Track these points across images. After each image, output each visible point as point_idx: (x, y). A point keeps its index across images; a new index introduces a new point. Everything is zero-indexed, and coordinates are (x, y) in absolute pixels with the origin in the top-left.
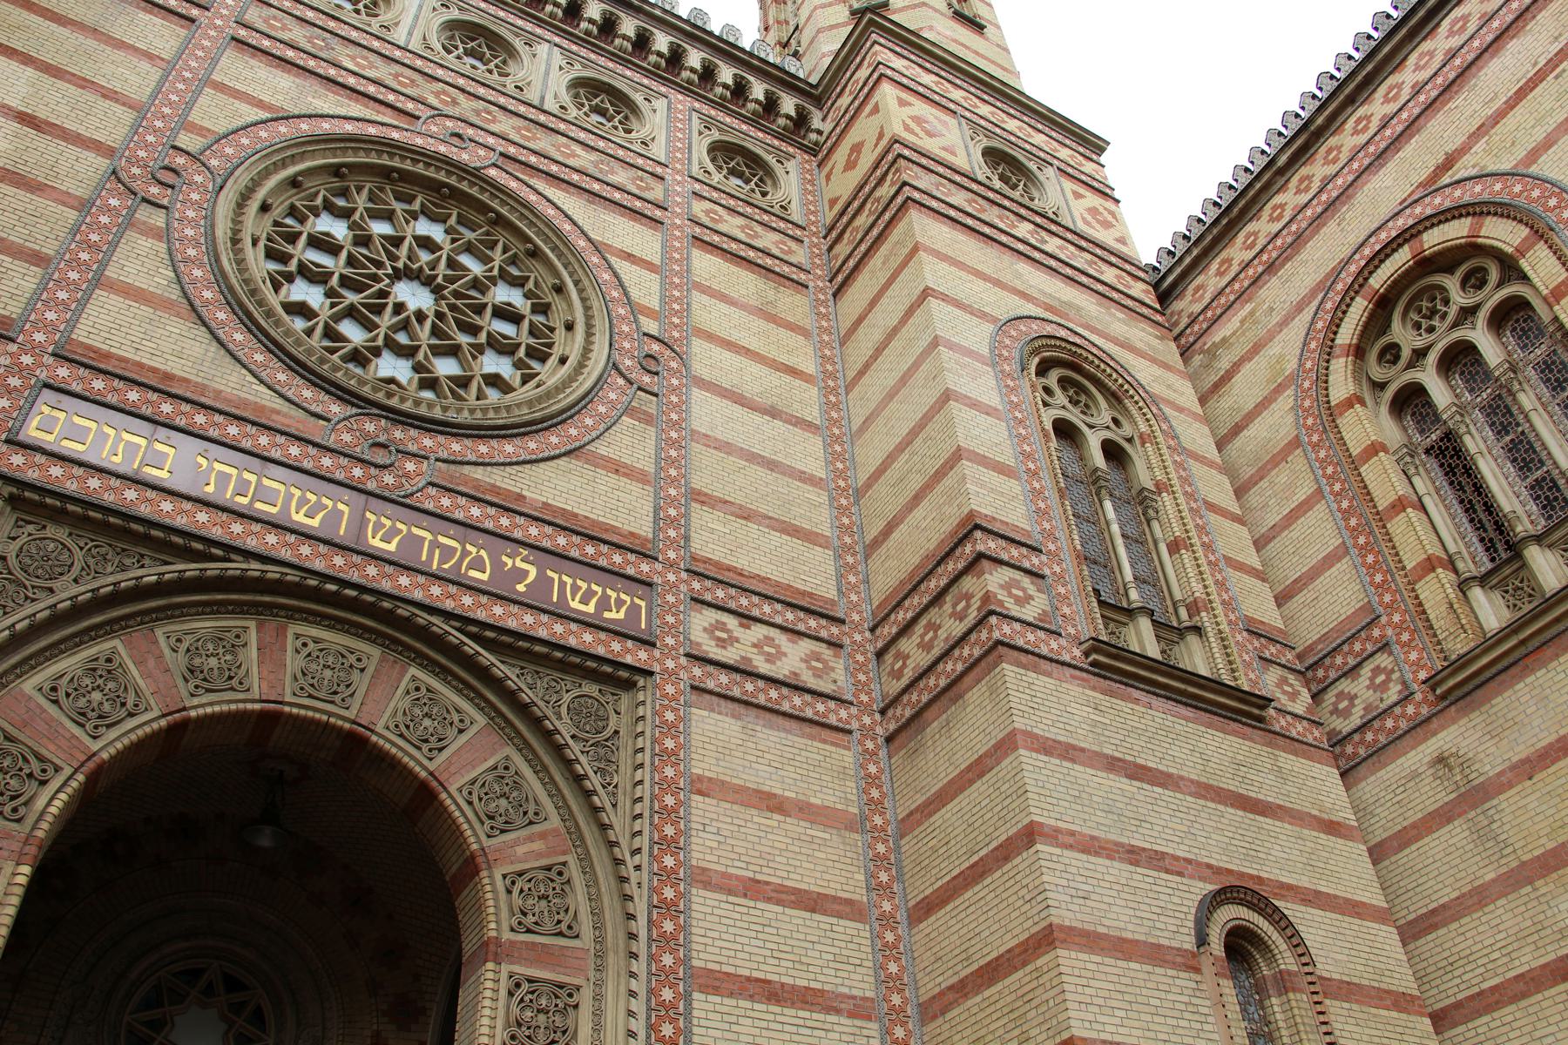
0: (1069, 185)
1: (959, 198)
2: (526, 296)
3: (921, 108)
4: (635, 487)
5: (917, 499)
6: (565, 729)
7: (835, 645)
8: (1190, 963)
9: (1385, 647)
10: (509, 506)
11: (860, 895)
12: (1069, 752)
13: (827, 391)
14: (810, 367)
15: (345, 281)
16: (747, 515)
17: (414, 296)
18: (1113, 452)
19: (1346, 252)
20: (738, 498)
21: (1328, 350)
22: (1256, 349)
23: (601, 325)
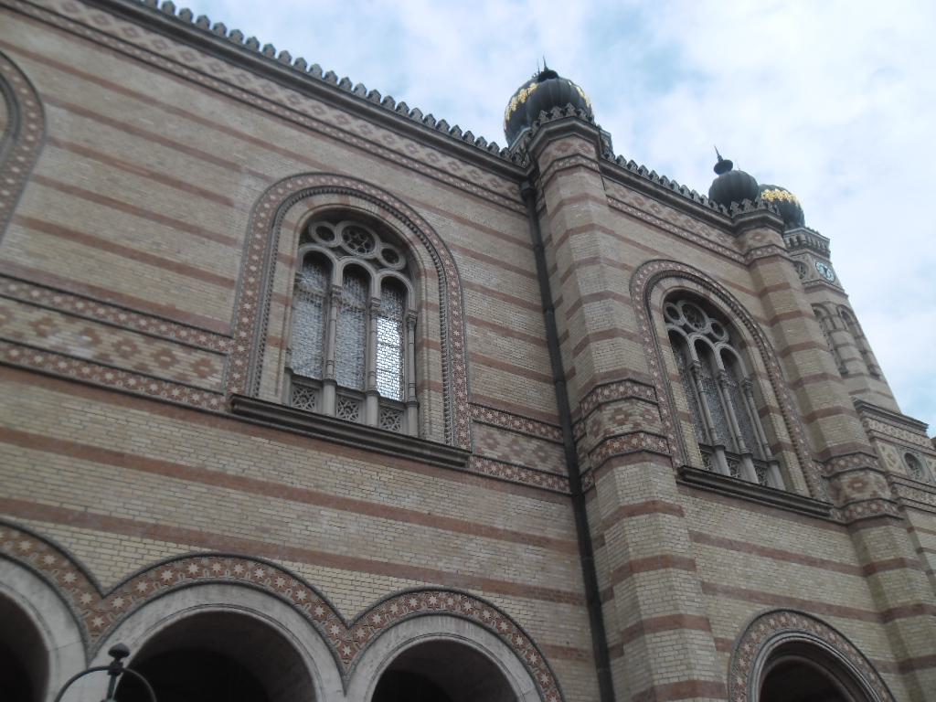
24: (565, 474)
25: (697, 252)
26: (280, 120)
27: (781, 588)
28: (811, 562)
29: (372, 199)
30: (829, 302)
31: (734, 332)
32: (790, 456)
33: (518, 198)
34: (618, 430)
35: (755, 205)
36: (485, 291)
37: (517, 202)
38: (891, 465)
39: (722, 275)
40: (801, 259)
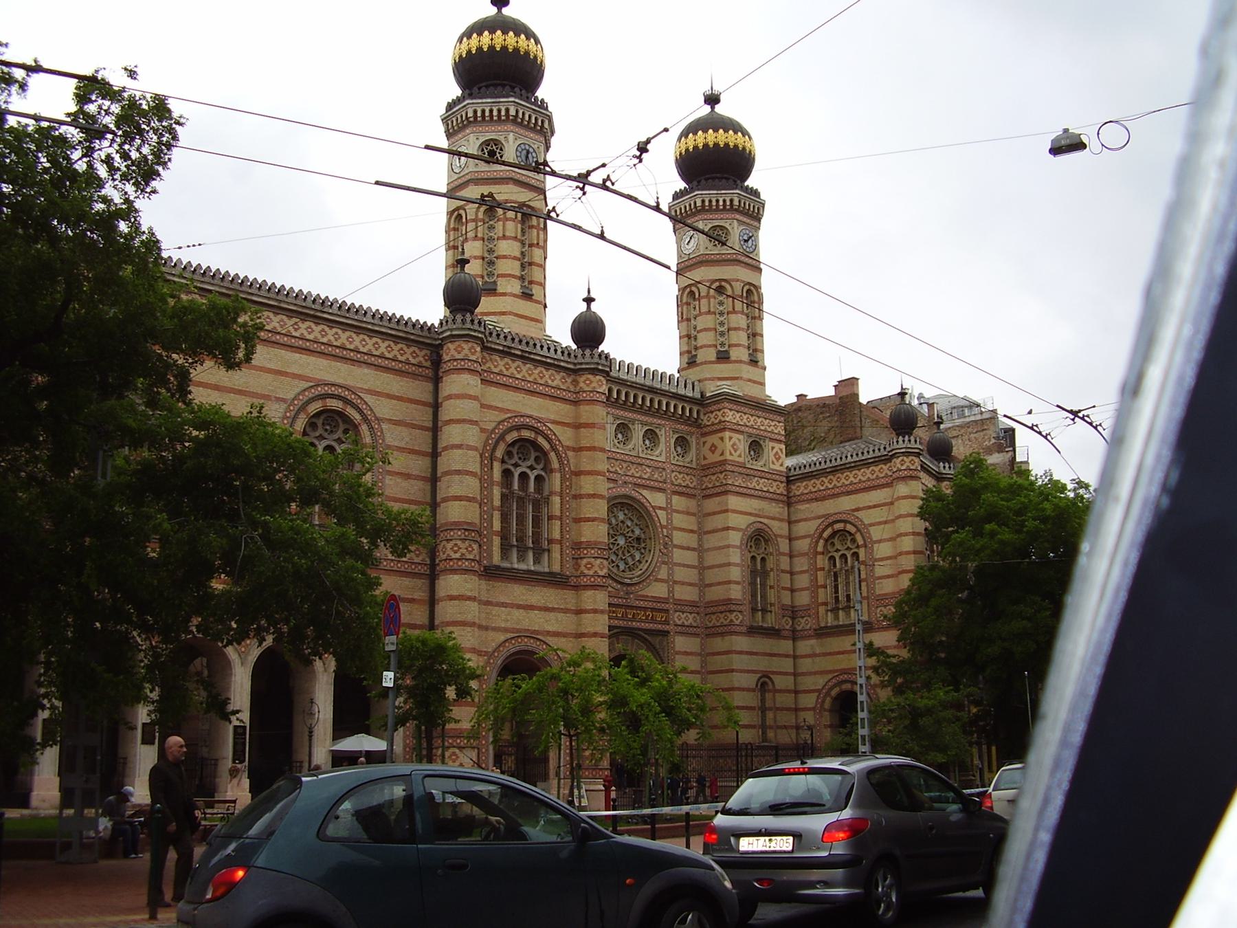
0: (771, 444)
1: (739, 482)
2: (641, 529)
3: (736, 436)
4: (665, 585)
5: (719, 584)
6: (658, 647)
7: (698, 613)
8: (753, 690)
9: (809, 616)
10: (645, 598)
11: (699, 669)
12: (741, 653)
13: (700, 535)
14: (695, 528)
15: (612, 543)
16: (683, 583)
17: (621, 541)
18: (763, 559)
19: (832, 512)
20: (681, 579)
21: (820, 536)
22: (805, 520)
23: (656, 537)
24: (428, 562)
25: (540, 400)
26: (289, 349)
27: (525, 624)
28: (547, 609)
29: (339, 397)
30: (738, 280)
31: (548, 462)
32: (556, 548)
33: (428, 364)
34: (454, 556)
35: (592, 355)
36: (401, 449)
37: (427, 368)
38: (731, 454)
39: (552, 417)
40: (727, 225)
